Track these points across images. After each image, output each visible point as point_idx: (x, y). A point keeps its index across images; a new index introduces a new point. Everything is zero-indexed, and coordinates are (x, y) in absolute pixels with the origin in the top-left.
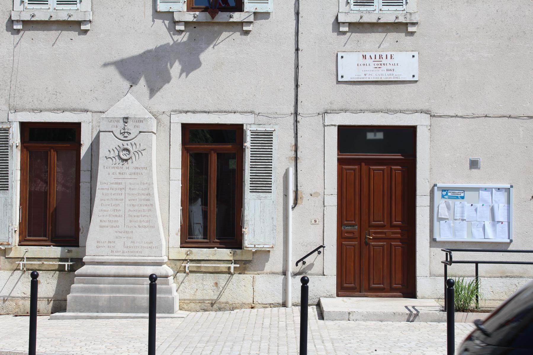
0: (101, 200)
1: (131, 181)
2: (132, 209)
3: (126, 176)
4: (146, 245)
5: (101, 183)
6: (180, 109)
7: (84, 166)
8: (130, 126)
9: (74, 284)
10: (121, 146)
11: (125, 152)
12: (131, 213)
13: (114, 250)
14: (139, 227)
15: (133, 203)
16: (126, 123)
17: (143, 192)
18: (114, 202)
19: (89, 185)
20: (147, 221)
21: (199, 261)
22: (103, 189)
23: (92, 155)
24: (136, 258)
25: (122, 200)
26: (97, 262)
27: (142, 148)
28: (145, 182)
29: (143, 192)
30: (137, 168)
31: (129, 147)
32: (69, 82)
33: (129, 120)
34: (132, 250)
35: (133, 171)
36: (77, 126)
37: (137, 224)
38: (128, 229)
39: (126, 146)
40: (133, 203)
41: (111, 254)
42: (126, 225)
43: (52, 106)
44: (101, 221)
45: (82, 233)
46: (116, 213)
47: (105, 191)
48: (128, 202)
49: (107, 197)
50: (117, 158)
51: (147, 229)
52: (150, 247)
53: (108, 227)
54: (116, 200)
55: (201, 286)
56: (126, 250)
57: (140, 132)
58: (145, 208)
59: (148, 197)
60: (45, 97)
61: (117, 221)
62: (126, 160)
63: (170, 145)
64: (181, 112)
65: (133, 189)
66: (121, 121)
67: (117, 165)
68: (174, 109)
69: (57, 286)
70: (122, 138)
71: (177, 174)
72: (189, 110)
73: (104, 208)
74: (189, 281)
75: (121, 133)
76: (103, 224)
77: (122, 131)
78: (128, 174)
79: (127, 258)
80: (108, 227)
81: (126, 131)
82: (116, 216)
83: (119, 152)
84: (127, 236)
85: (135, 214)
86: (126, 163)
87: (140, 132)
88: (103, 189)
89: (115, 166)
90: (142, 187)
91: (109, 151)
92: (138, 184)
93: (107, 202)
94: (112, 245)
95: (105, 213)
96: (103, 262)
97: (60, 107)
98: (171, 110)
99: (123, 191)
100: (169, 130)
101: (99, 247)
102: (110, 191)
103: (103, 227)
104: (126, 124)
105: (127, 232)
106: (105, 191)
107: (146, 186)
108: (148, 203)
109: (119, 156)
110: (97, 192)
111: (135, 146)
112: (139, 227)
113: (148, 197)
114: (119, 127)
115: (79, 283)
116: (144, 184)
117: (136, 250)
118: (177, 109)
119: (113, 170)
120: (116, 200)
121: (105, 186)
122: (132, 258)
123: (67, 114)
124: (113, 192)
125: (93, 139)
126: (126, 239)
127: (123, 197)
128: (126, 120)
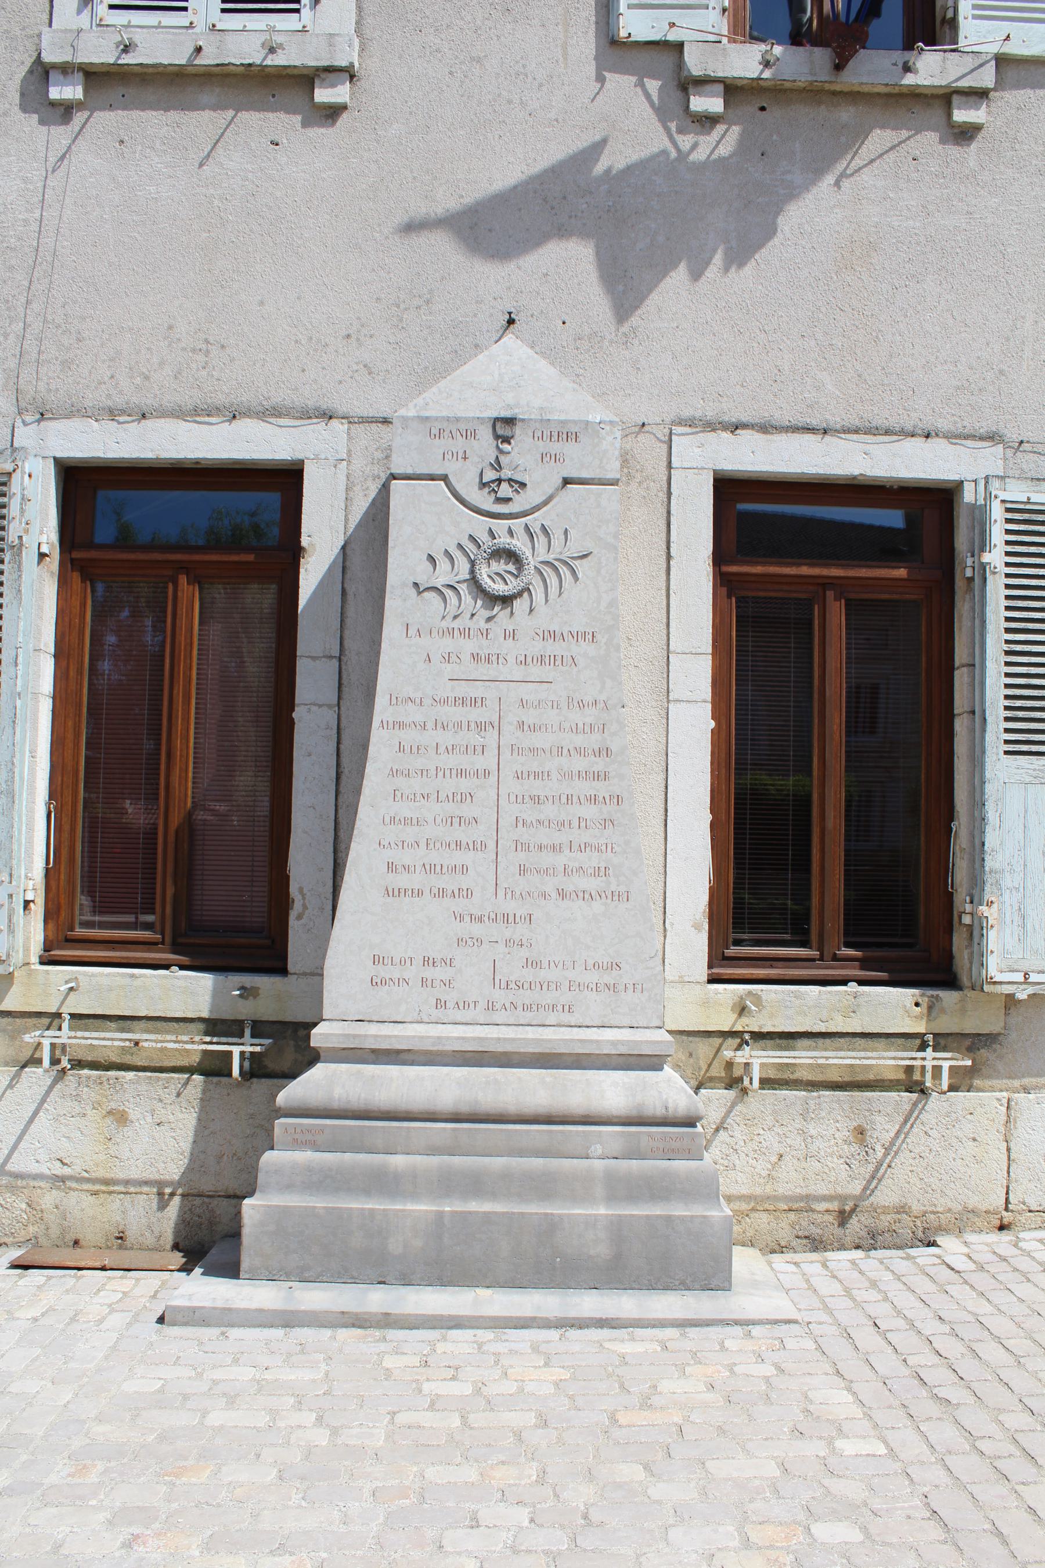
0: (394, 773)
1: (525, 691)
2: (530, 813)
3: (505, 671)
4: (592, 977)
5: (394, 700)
6: (710, 415)
7: (312, 639)
8: (522, 456)
9: (272, 1149)
10: (483, 537)
11: (500, 566)
12: (524, 834)
13: (451, 997)
14: (562, 894)
15: (536, 787)
16: (507, 440)
17: (579, 740)
18: (449, 785)
19: (331, 716)
20: (596, 872)
21: (788, 1038)
22: (401, 725)
23: (344, 592)
24: (547, 1034)
25: (487, 773)
26: (373, 1051)
27: (574, 548)
28: (588, 699)
29: (579, 740)
30: (553, 635)
31: (520, 544)
32: (262, 303)
33: (518, 430)
34: (527, 996)
35: (537, 647)
36: (286, 480)
37: (550, 885)
38: (510, 906)
39: (503, 540)
40: (536, 787)
41: (436, 1014)
42: (503, 884)
43: (188, 398)
44: (391, 867)
45: (299, 917)
46: (460, 834)
47: (409, 736)
48: (510, 785)
49: (419, 763)
50: (463, 588)
51: (597, 906)
52: (612, 988)
53: (420, 893)
54: (461, 773)
55: (797, 1141)
56: (500, 996)
57: (566, 482)
58: (589, 812)
59: (599, 764)
60: (162, 364)
61: (465, 869)
62: (506, 600)
63: (669, 557)
64: (711, 426)
65: (533, 729)
66: (485, 434)
67: (464, 622)
68: (687, 413)
69: (196, 1135)
70: (488, 505)
71: (695, 675)
72: (745, 418)
73: (405, 810)
74: (749, 1121)
75: (483, 485)
76: (402, 880)
77: (490, 475)
78: (511, 660)
79: (509, 1033)
80: (420, 893)
81: (506, 473)
82: (458, 844)
83: (473, 563)
84: (508, 934)
85: (544, 836)
86: (501, 614)
87: (566, 482)
88: (401, 725)
89: (456, 624)
90: (576, 717)
91: (431, 559)
92: (555, 705)
93: (416, 784)
94: (439, 973)
95: (410, 833)
96: (399, 1052)
97: (220, 399)
98: (672, 416)
99: (492, 735)
100: (662, 495)
101: (383, 982)
102: (431, 737)
103: (402, 892)
104: (506, 447)
105: (506, 918)
106: (409, 736)
107: (590, 715)
108: (601, 789)
109: (474, 581)
110: (373, 739)
111: (543, 539)
112: (562, 894)
113: (599, 764)
114: (473, 458)
115: (297, 1144)
116: (581, 705)
117: (549, 997)
118: (698, 414)
119: (447, 644)
120: (461, 773)
121: (413, 714)
122: (531, 1033)
123: (247, 426)
124: (446, 738)
125: (352, 526)
126: (501, 948)
127: (488, 761)
128: (504, 428)
